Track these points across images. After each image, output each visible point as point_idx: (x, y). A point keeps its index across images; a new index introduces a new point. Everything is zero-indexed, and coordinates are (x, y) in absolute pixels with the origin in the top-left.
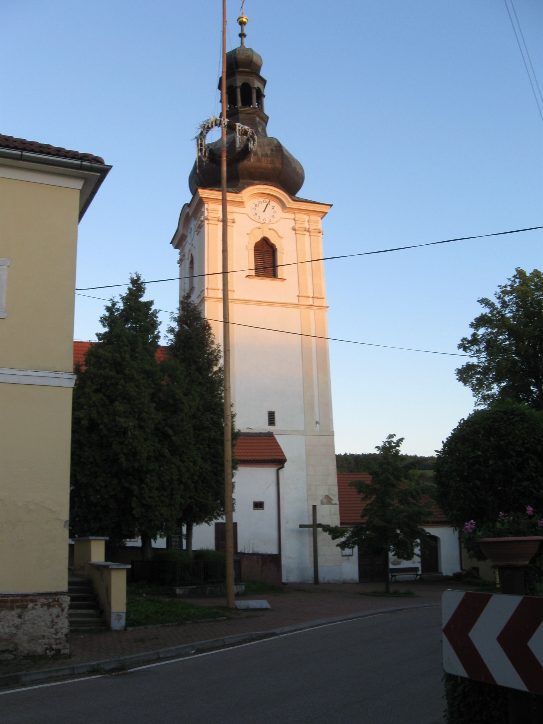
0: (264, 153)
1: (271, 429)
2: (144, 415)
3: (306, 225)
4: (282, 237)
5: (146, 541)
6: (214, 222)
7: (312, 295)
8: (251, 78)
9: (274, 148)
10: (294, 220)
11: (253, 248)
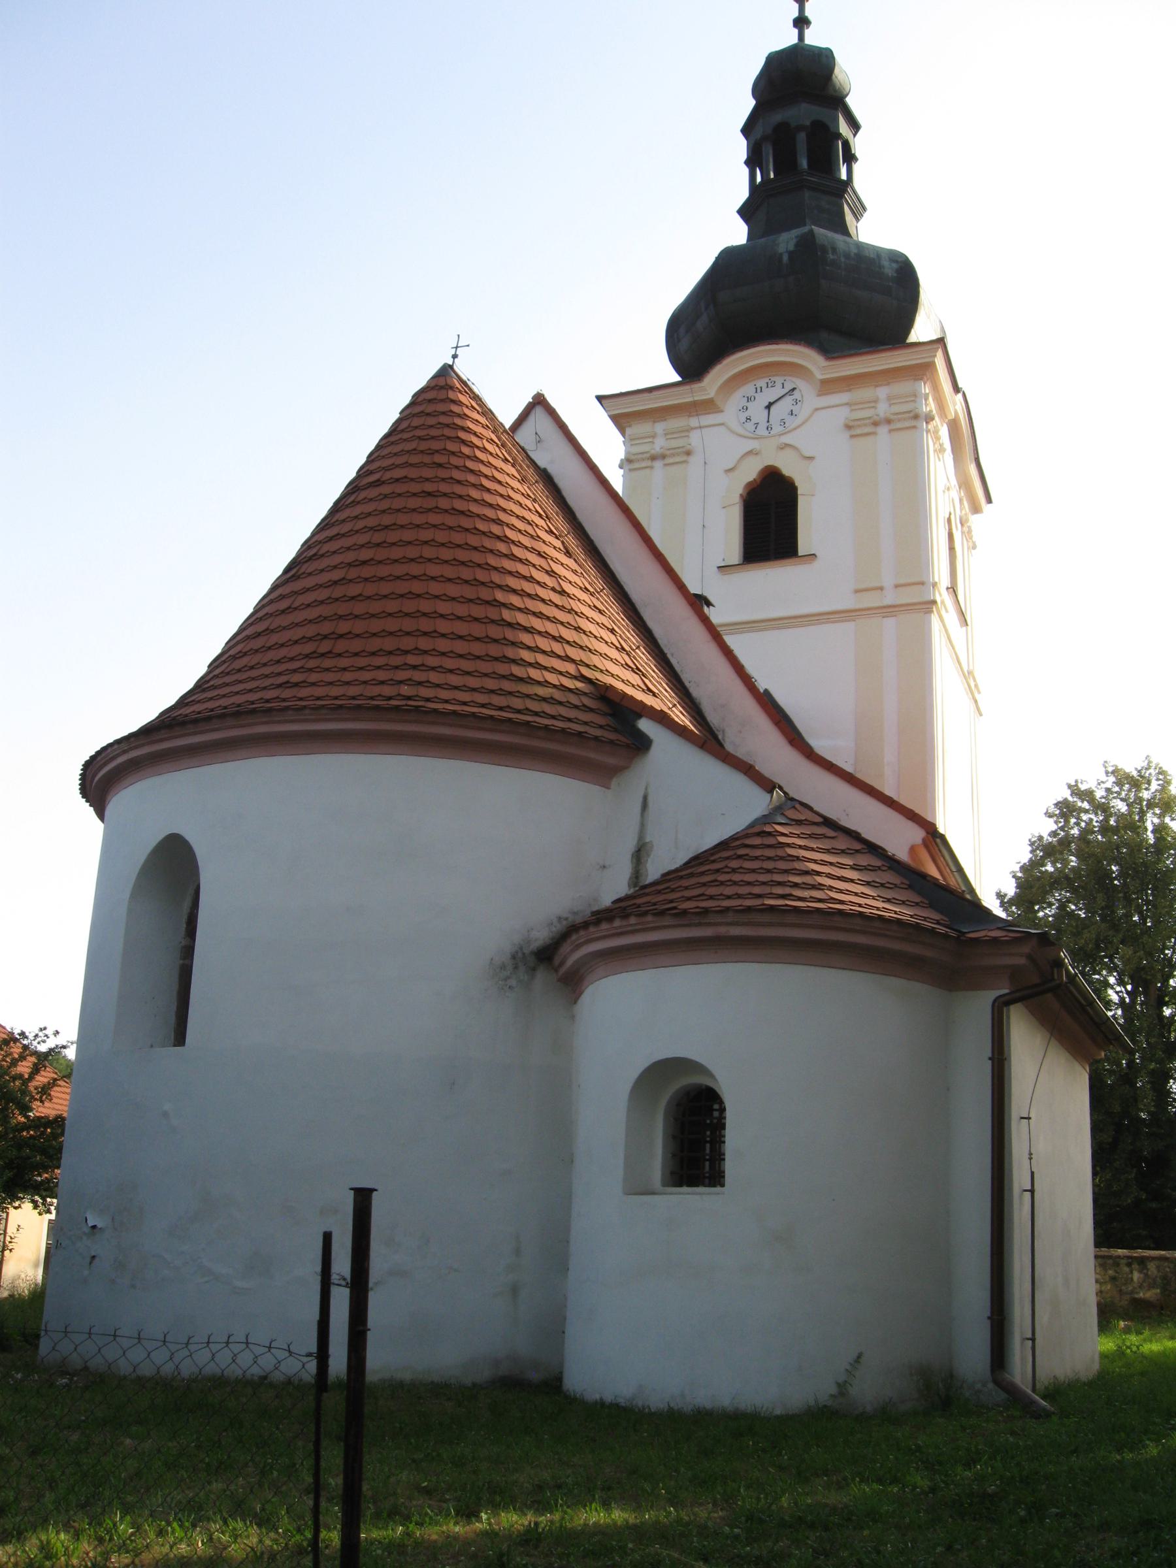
4: (811, 458)
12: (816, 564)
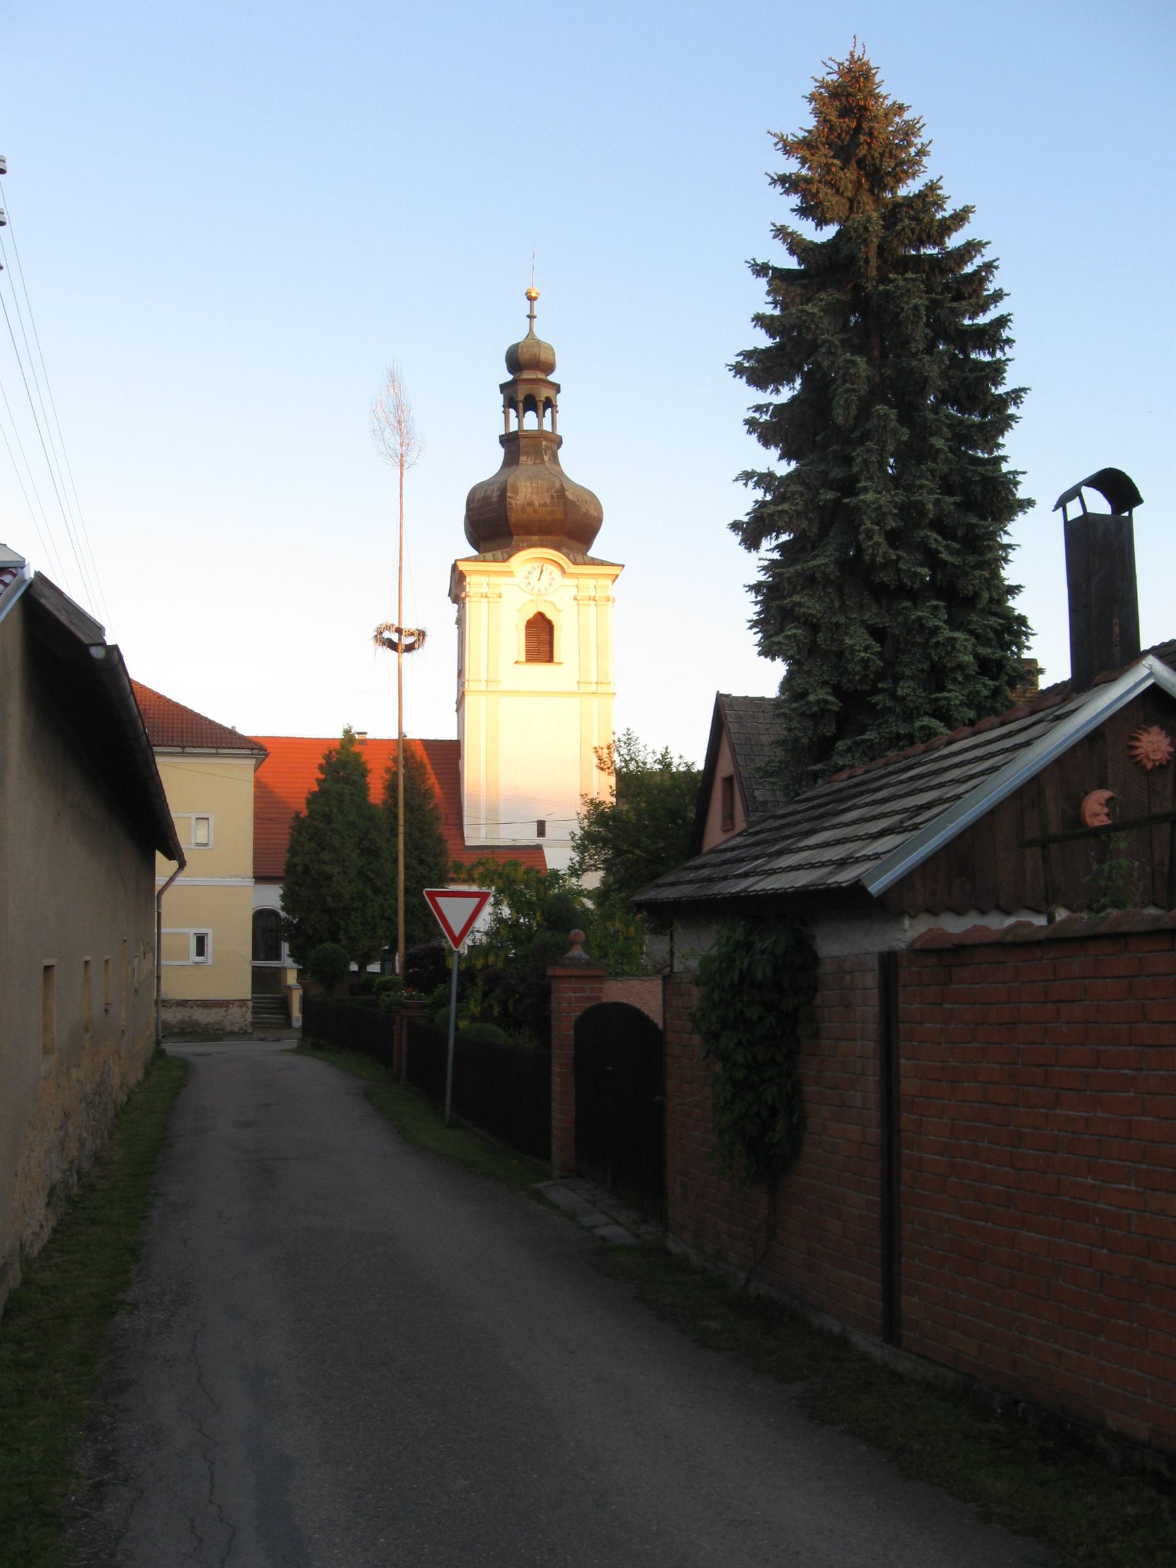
0: (542, 502)
1: (540, 841)
2: (346, 863)
3: (592, 593)
5: (362, 967)
6: (477, 599)
7: (594, 680)
8: (535, 386)
9: (555, 494)
10: (577, 587)
11: (524, 628)
12: (562, 666)
